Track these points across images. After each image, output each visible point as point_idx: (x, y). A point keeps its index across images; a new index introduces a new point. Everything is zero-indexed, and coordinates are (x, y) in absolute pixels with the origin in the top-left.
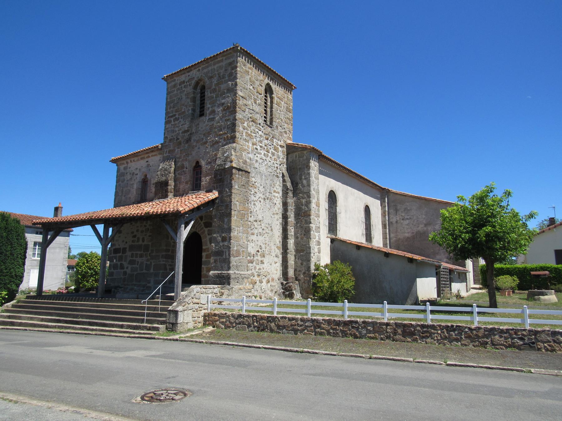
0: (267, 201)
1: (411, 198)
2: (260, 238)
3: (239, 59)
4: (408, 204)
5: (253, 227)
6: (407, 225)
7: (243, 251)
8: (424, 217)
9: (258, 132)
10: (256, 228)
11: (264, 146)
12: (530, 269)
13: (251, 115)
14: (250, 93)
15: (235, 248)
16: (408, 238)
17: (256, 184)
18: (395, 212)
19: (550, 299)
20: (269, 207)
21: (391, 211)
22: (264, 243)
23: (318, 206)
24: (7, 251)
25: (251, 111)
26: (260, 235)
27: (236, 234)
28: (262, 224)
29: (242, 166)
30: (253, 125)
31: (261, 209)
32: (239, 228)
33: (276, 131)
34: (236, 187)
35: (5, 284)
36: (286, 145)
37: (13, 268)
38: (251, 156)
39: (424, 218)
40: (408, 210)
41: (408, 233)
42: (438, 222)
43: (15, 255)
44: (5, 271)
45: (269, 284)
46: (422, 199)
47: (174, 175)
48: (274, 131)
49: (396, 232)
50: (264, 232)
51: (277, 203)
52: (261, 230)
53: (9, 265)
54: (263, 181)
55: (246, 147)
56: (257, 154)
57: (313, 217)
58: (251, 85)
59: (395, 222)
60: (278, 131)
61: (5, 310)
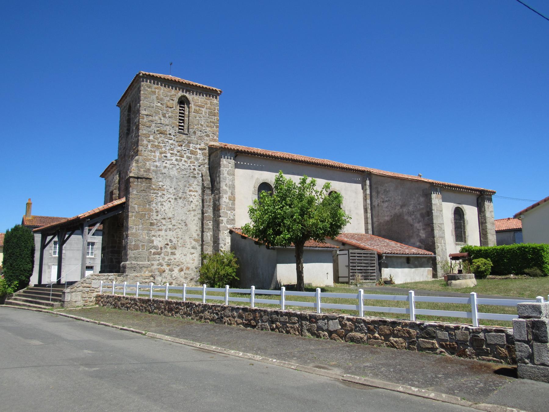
0: (180, 201)
1: (389, 179)
2: (170, 233)
3: (142, 83)
4: (387, 185)
5: (159, 224)
6: (386, 207)
7: (143, 245)
8: (400, 197)
9: (167, 142)
10: (164, 225)
11: (176, 152)
12: (508, 250)
13: (159, 128)
14: (157, 109)
15: (133, 243)
16: (388, 221)
17: (164, 187)
18: (377, 194)
19: (461, 284)
20: (183, 205)
21: (374, 194)
22: (175, 237)
23: (232, 199)
24: (17, 253)
25: (159, 125)
26: (170, 230)
27: (134, 231)
28: (172, 221)
29: (142, 173)
30: (161, 137)
31: (172, 208)
32: (137, 227)
33: (193, 137)
34: (135, 192)
35: (17, 276)
36: (208, 147)
37: (22, 264)
38: (158, 164)
39: (400, 199)
40: (387, 192)
41: (387, 216)
42: (411, 203)
43: (23, 255)
44: (16, 267)
45: (182, 273)
46: (397, 178)
47: (118, 186)
48: (190, 137)
49: (378, 216)
50: (175, 227)
51: (195, 201)
52: (171, 226)
53: (19, 262)
54: (174, 183)
55: (152, 157)
56: (166, 161)
57: (223, 210)
58: (159, 102)
59: (377, 205)
60: (197, 136)
61: (18, 294)
